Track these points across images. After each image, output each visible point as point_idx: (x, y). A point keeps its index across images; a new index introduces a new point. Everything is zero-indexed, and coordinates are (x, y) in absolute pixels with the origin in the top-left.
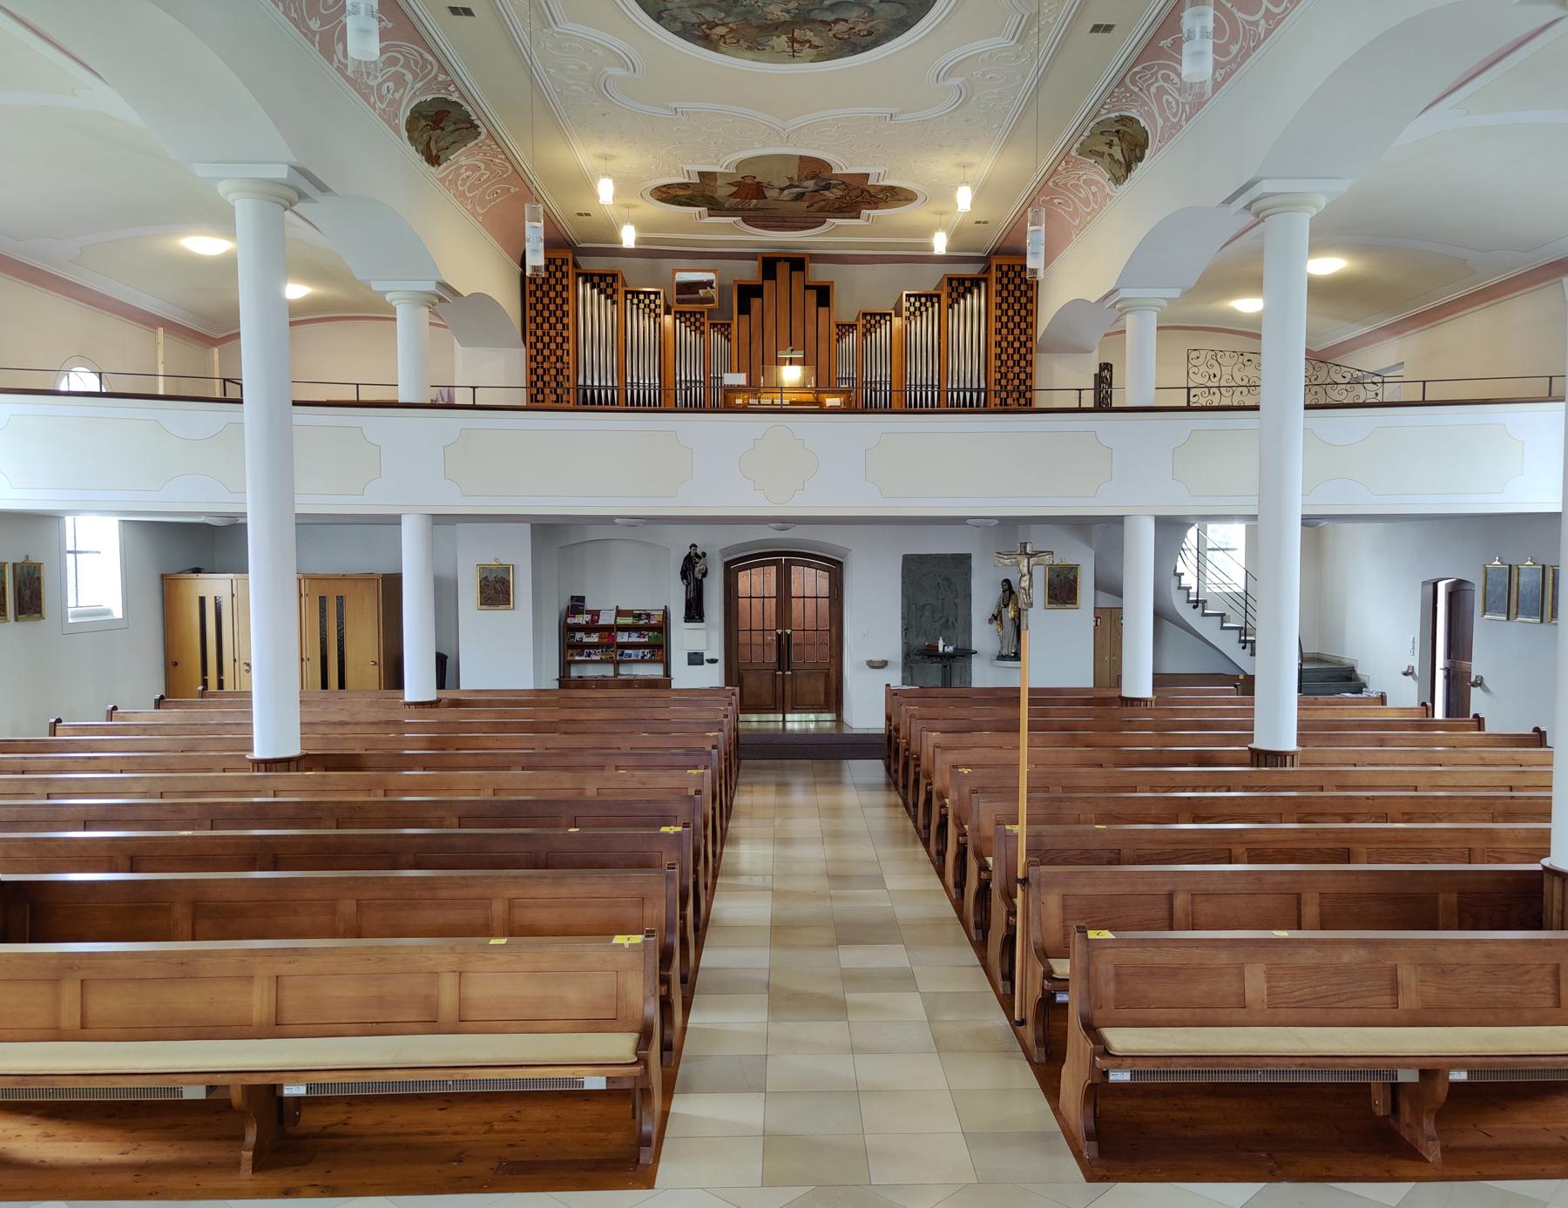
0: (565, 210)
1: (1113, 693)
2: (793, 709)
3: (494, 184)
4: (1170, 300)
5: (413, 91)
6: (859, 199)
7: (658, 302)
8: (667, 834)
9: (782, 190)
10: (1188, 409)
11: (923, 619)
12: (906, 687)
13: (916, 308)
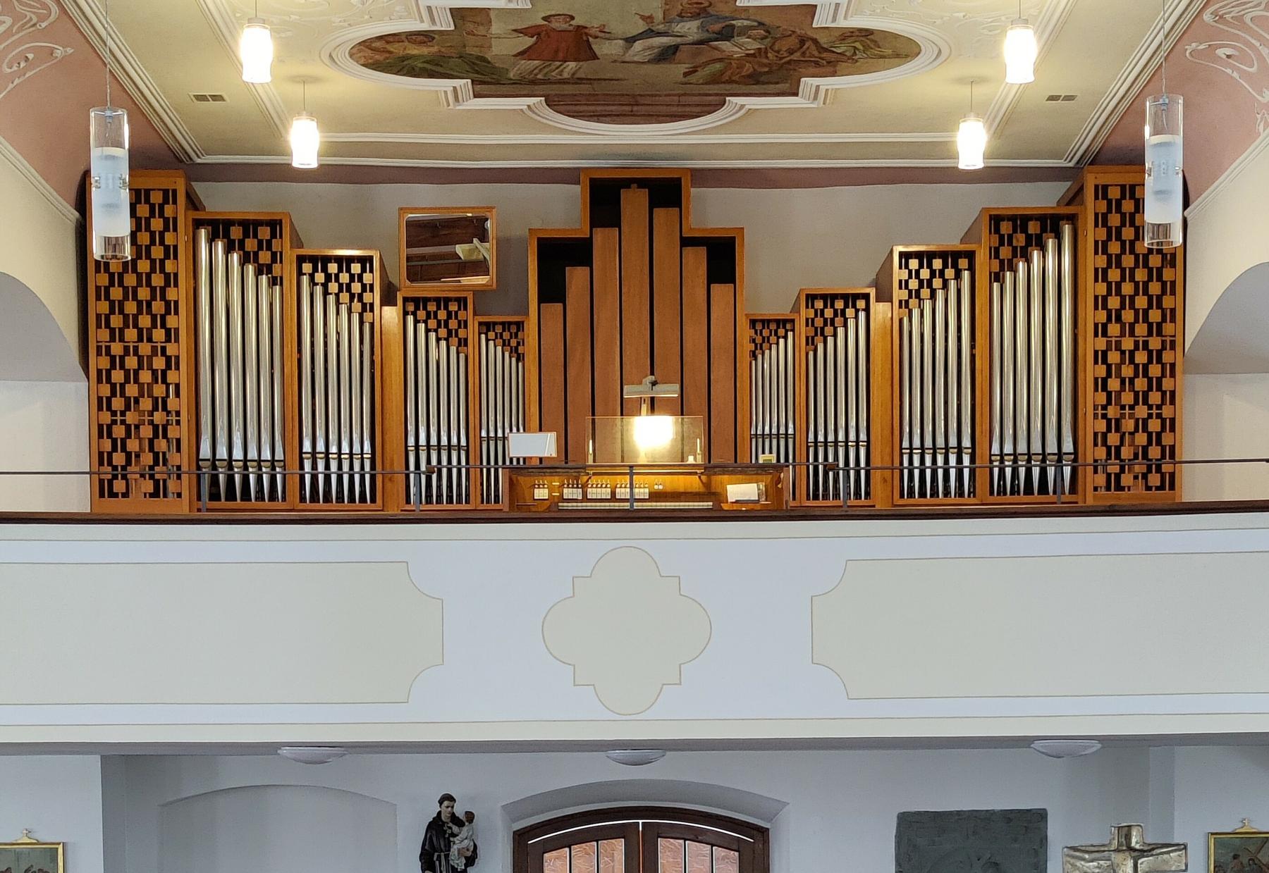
3: (20, 42)
6: (796, 56)
7: (367, 278)
9: (631, 40)
13: (921, 282)
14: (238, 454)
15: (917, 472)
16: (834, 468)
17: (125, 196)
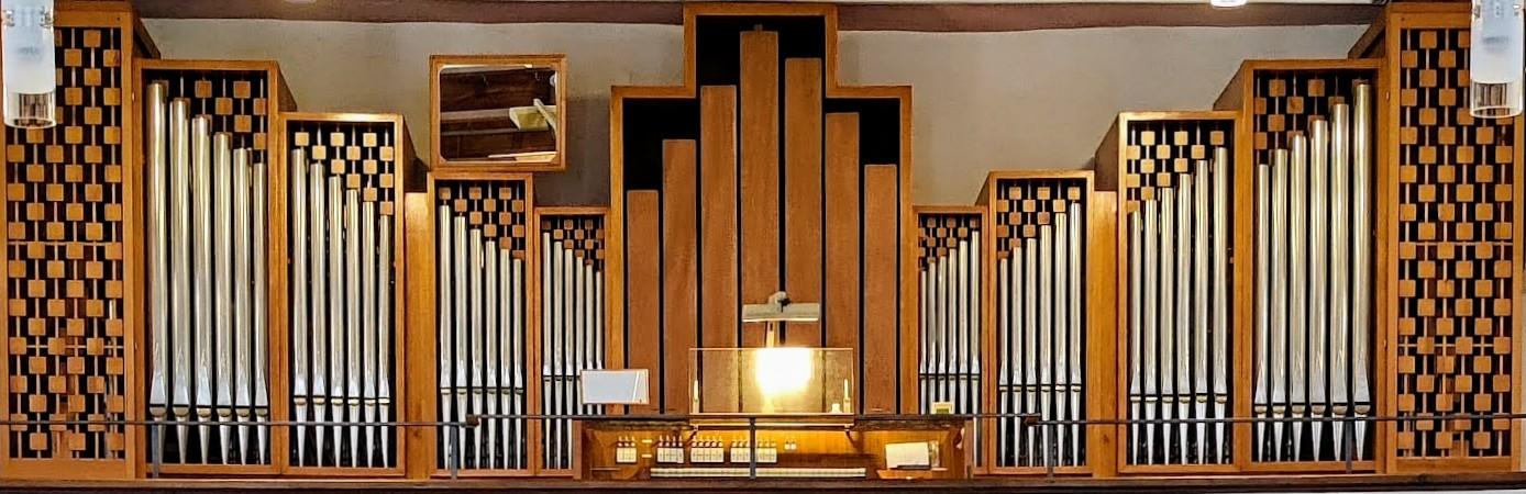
7: (386, 153)
13: (1158, 164)
14: (204, 397)
16: (1036, 421)
17: (48, 37)
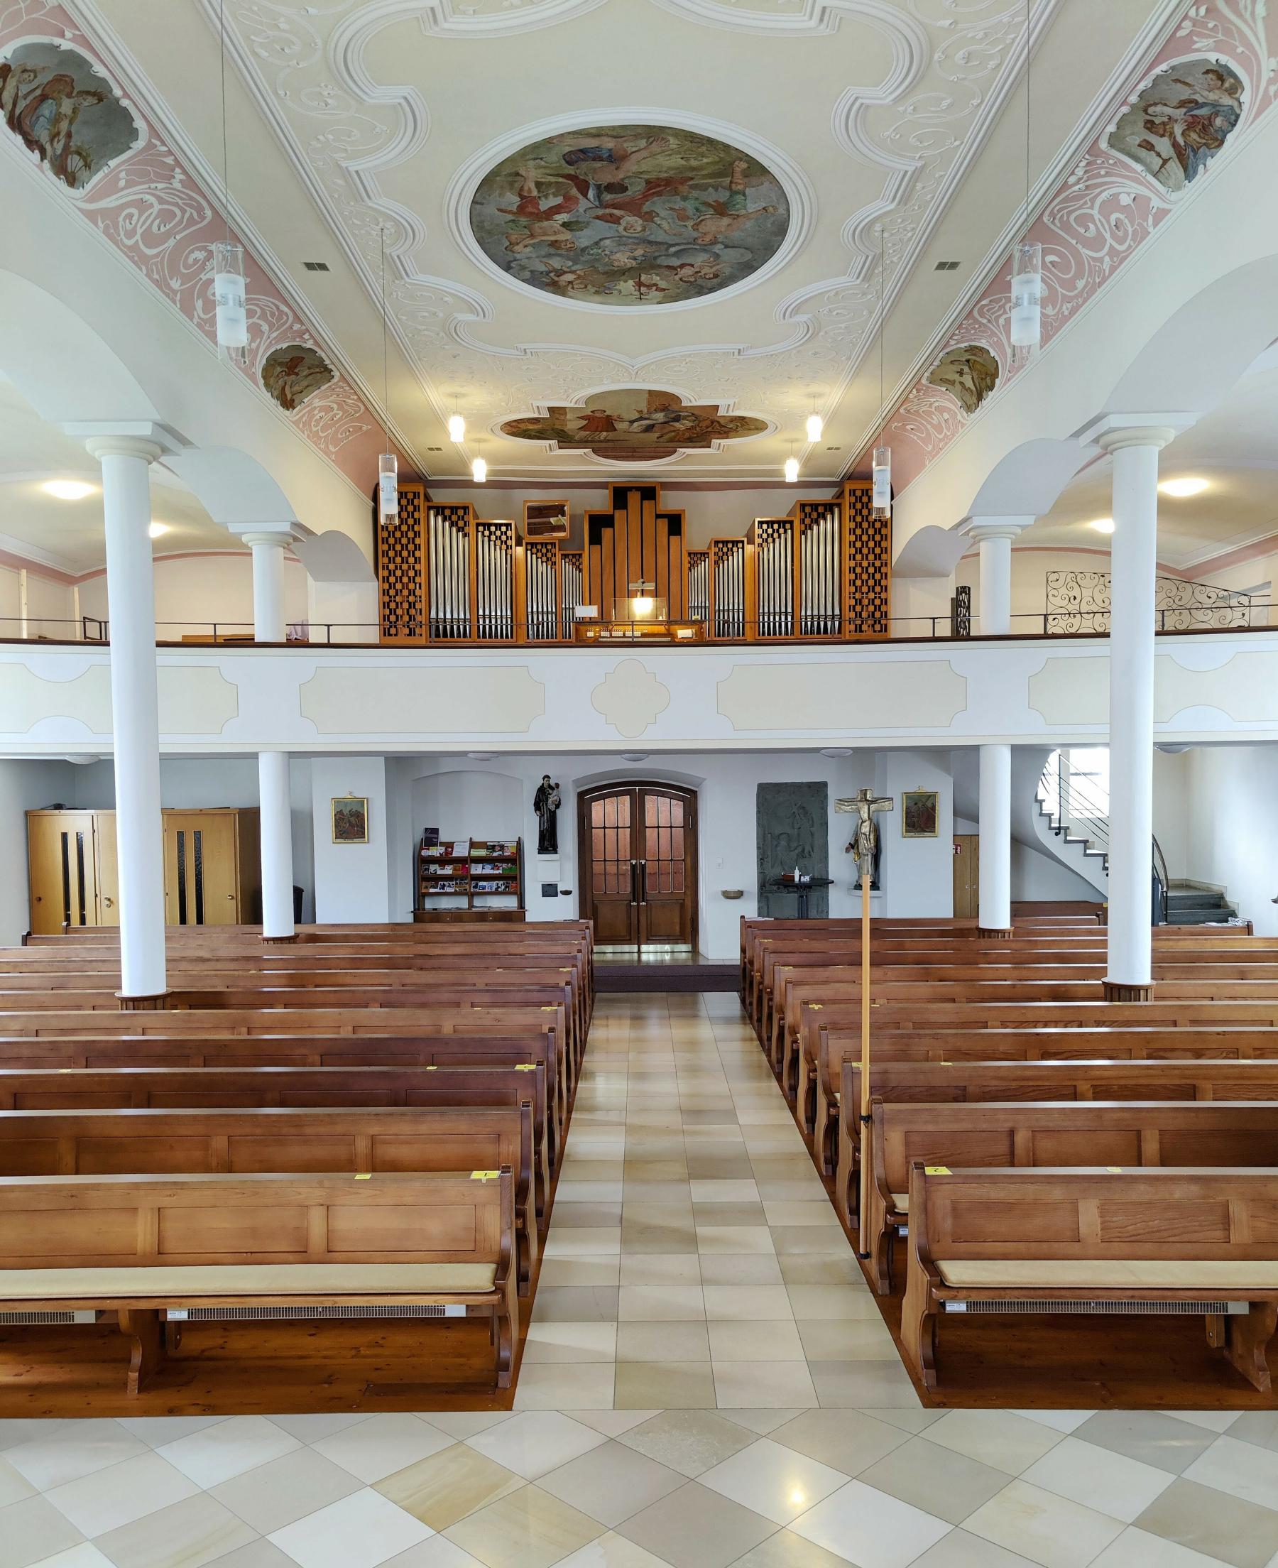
0: (416, 444)
1: (970, 924)
2: (648, 940)
3: (343, 425)
4: (1023, 527)
5: (269, 341)
6: (709, 430)
7: (509, 533)
8: (522, 1072)
9: (632, 422)
10: (1046, 636)
11: (779, 849)
12: (761, 919)
13: (768, 535)
14: (448, 616)
15: (766, 624)
16: (728, 622)
17: (395, 495)
